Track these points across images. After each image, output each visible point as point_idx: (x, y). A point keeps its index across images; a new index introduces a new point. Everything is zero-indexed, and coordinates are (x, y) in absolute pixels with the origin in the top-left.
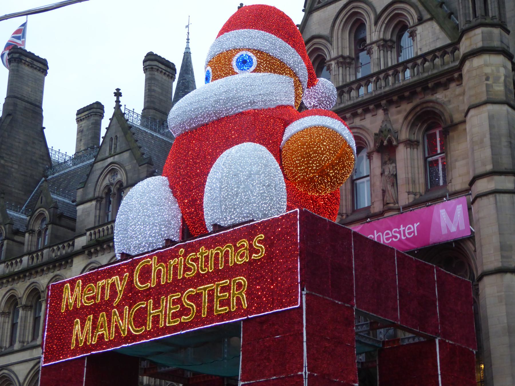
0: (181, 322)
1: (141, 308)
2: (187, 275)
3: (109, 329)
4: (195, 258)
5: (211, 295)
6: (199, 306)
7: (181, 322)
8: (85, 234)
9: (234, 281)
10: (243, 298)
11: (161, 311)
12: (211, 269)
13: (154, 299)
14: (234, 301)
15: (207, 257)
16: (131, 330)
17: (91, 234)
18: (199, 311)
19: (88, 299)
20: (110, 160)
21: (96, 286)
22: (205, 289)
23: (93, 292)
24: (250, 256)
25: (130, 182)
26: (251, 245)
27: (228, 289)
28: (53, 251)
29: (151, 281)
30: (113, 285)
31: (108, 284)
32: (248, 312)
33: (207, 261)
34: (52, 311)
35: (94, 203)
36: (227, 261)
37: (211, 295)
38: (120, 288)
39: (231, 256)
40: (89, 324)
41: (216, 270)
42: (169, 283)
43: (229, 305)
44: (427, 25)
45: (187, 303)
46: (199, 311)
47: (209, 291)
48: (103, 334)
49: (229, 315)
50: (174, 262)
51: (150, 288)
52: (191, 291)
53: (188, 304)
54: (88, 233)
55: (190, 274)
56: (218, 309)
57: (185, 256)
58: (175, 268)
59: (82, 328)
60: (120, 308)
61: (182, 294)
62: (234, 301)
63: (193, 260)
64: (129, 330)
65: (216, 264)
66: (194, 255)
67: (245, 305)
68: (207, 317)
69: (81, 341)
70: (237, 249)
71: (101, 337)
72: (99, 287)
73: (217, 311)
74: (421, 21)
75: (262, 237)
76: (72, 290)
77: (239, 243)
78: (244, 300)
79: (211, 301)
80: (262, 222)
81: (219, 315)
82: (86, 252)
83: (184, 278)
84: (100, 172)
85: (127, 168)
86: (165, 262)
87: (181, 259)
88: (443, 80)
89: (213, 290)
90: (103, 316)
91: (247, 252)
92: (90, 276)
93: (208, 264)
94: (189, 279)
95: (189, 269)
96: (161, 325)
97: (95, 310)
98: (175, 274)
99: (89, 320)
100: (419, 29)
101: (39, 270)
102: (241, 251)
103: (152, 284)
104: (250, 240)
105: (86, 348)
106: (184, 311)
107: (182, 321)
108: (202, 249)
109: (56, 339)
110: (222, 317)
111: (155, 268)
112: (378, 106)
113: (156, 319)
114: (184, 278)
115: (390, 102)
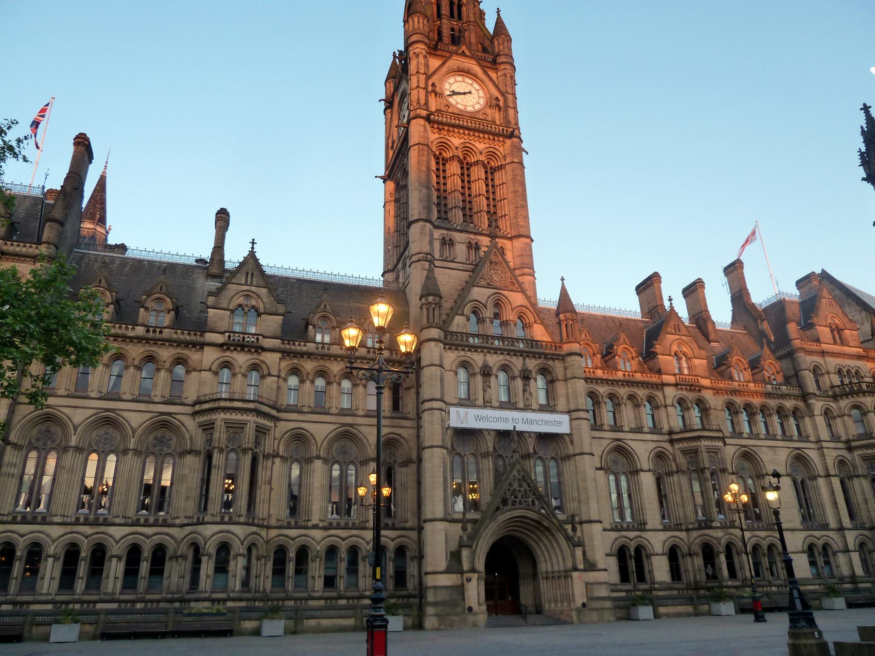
8: (223, 333)
17: (229, 336)
20: (248, 288)
25: (267, 311)
28: (176, 333)
35: (228, 313)
44: (540, 325)
54: (227, 334)
74: (535, 322)
82: (225, 348)
84: (235, 292)
85: (264, 300)
88: (555, 357)
100: (535, 326)
101: (160, 343)
112: (521, 355)
115: (528, 356)
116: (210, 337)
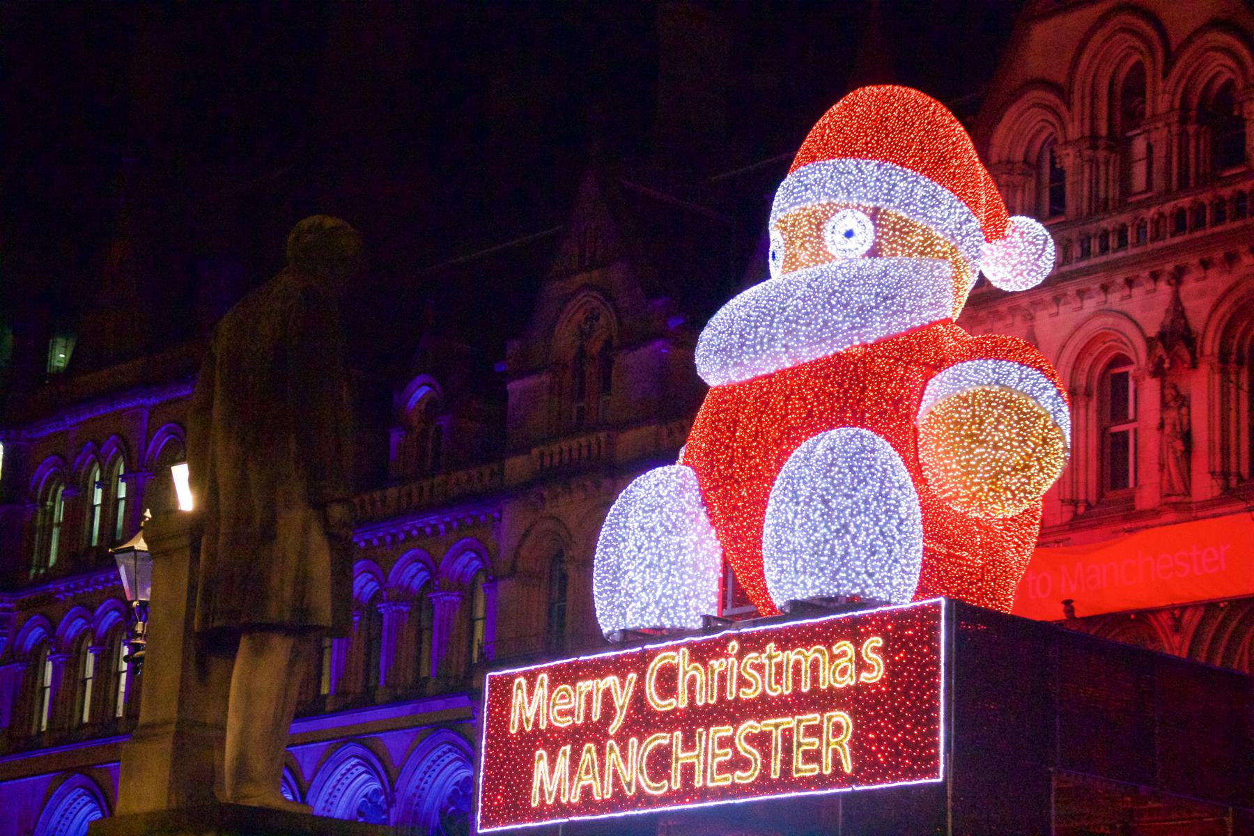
0: (733, 784)
1: (660, 745)
2: (744, 693)
3: (602, 777)
4: (758, 664)
5: (787, 736)
6: (766, 756)
7: (733, 784)
9: (829, 720)
10: (844, 750)
11: (698, 756)
12: (787, 689)
13: (684, 732)
14: (827, 759)
15: (779, 666)
16: (643, 785)
17: (542, 455)
18: (766, 766)
19: (561, 713)
21: (575, 691)
22: (777, 726)
23: (570, 702)
24: (858, 675)
26: (858, 654)
27: (818, 732)
29: (677, 694)
30: (607, 694)
31: (598, 690)
32: (851, 780)
33: (779, 673)
34: (493, 727)
35: (545, 378)
36: (815, 679)
37: (787, 736)
39: (824, 668)
40: (563, 763)
41: (796, 693)
42: (710, 705)
43: (820, 763)
45: (742, 747)
46: (766, 766)
47: (784, 730)
48: (590, 786)
49: (820, 781)
50: (720, 665)
51: (676, 709)
52: (752, 727)
53: (746, 751)
55: (749, 694)
56: (801, 766)
57: (740, 656)
58: (722, 678)
59: (552, 771)
60: (622, 738)
61: (735, 730)
62: (827, 759)
63: (754, 666)
64: (638, 786)
65: (797, 682)
66: (756, 658)
67: (848, 767)
68: (780, 777)
69: (550, 794)
70: (833, 658)
71: (587, 791)
72: (581, 693)
73: (798, 771)
75: (878, 642)
76: (530, 692)
77: (838, 648)
78: (845, 757)
79: (788, 750)
80: (878, 613)
81: (801, 778)
83: (737, 699)
86: (705, 664)
87: (733, 663)
89: (790, 730)
90: (589, 751)
91: (852, 668)
92: (564, 669)
93: (781, 679)
94: (749, 703)
95: (749, 685)
96: (698, 783)
98: (722, 689)
99: (564, 753)
102: (842, 662)
103: (681, 702)
104: (858, 645)
105: (560, 809)
106: (740, 763)
107: (737, 781)
108: (771, 647)
109: (503, 784)
110: (808, 783)
111: (685, 673)
113: (688, 771)
114: (737, 699)
116: (518, 467)
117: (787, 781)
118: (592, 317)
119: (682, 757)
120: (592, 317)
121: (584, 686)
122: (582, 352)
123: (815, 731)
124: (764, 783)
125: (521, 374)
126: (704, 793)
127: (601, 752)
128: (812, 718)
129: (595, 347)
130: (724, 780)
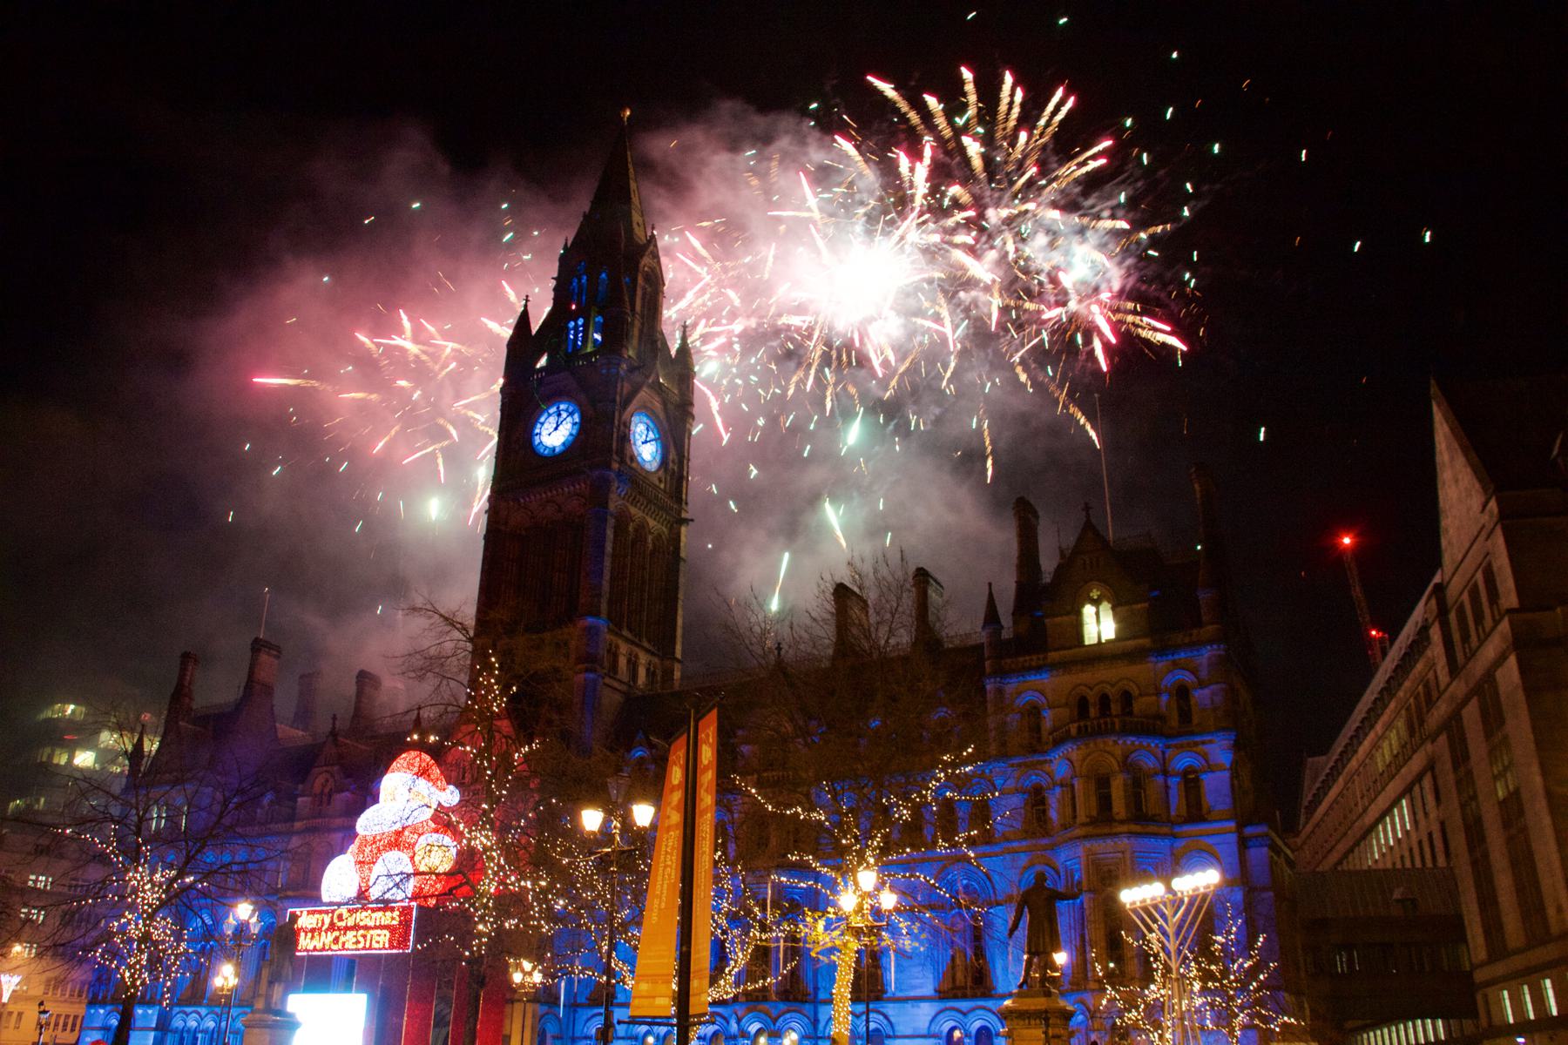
14: (381, 943)
38: (327, 921)
49: (380, 949)
55: (362, 924)
67: (387, 946)
97: (313, 930)
106: (358, 942)
116: (298, 825)
117: (370, 948)
118: (327, 781)
119: (342, 939)
120: (327, 781)
121: (317, 916)
122: (323, 791)
123: (379, 935)
124: (364, 948)
125: (302, 796)
126: (347, 950)
127: (320, 934)
128: (379, 931)
129: (327, 790)
130: (355, 947)
